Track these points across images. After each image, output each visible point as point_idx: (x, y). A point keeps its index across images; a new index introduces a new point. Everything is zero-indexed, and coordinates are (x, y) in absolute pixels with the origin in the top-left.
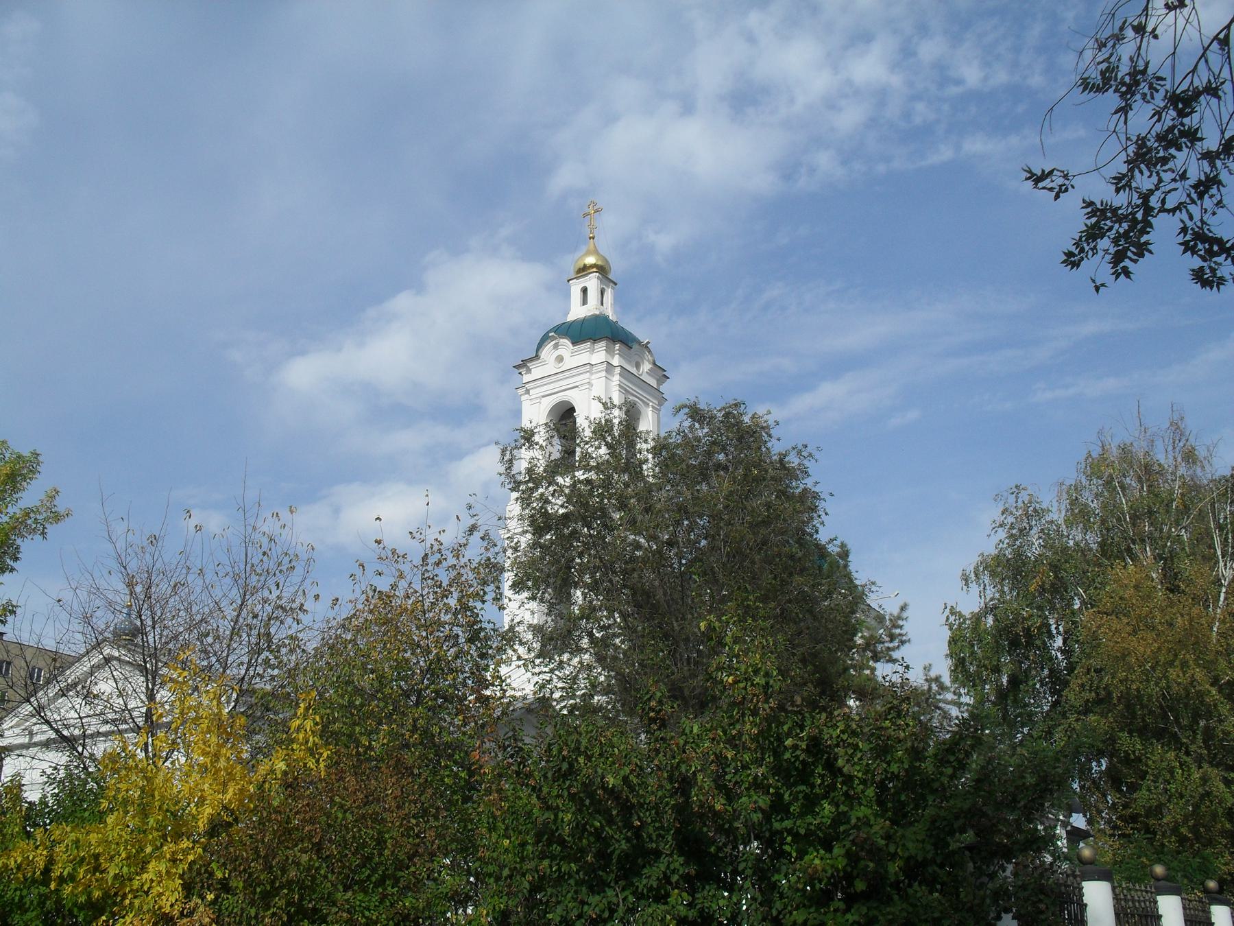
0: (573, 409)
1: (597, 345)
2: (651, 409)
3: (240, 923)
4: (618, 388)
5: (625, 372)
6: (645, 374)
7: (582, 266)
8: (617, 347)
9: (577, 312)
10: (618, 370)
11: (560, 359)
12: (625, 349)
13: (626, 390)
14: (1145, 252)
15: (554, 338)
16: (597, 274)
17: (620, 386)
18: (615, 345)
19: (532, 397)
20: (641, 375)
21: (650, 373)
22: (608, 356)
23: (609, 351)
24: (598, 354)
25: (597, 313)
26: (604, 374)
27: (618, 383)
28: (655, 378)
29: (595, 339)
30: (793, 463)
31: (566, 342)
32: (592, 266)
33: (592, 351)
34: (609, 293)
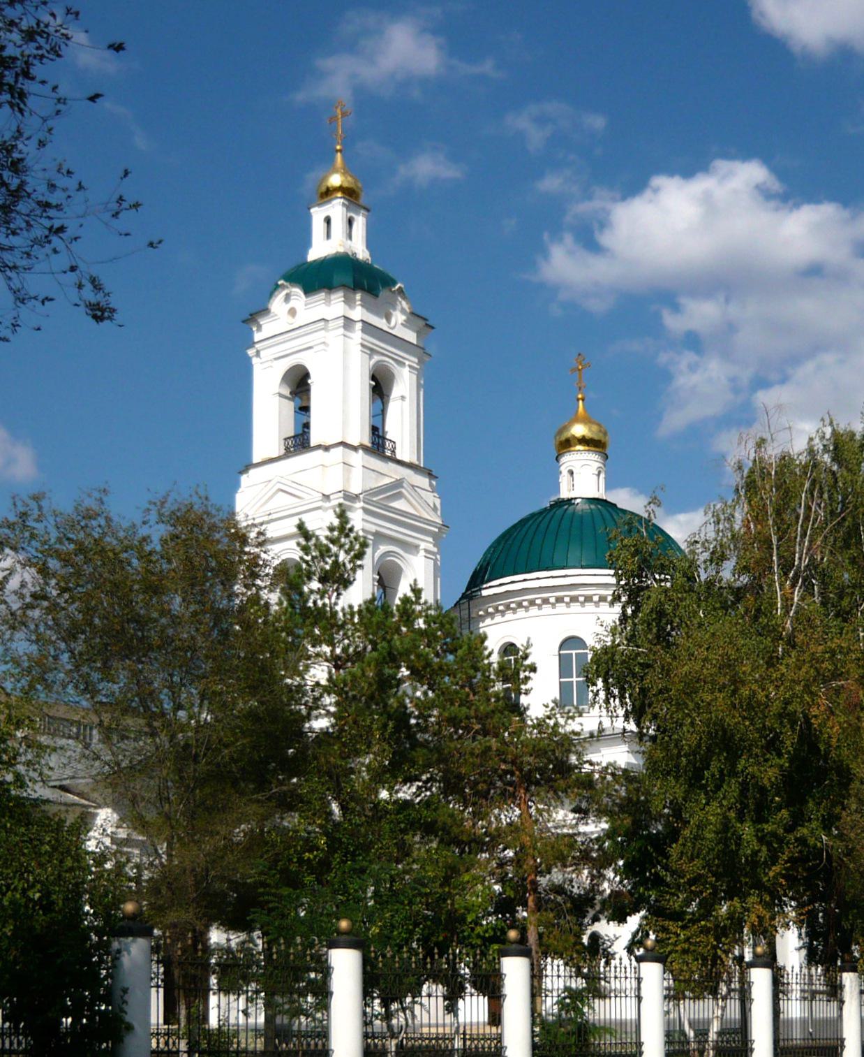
0: (306, 375)
1: (333, 297)
2: (407, 369)
3: (702, 1052)
4: (360, 348)
5: (368, 328)
6: (399, 326)
7: (323, 189)
8: (358, 296)
9: (320, 249)
10: (359, 326)
11: (292, 312)
12: (369, 298)
13: (371, 350)
14: (369, 445)
15: (283, 287)
16: (342, 200)
17: (362, 345)
18: (355, 294)
19: (263, 360)
20: (393, 328)
21: (407, 324)
22: (347, 307)
23: (349, 302)
24: (333, 306)
25: (341, 250)
26: (342, 331)
27: (360, 341)
28: (413, 330)
29: (329, 287)
30: (298, 544)
31: (297, 291)
32: (337, 189)
33: (328, 302)
34: (360, 222)
